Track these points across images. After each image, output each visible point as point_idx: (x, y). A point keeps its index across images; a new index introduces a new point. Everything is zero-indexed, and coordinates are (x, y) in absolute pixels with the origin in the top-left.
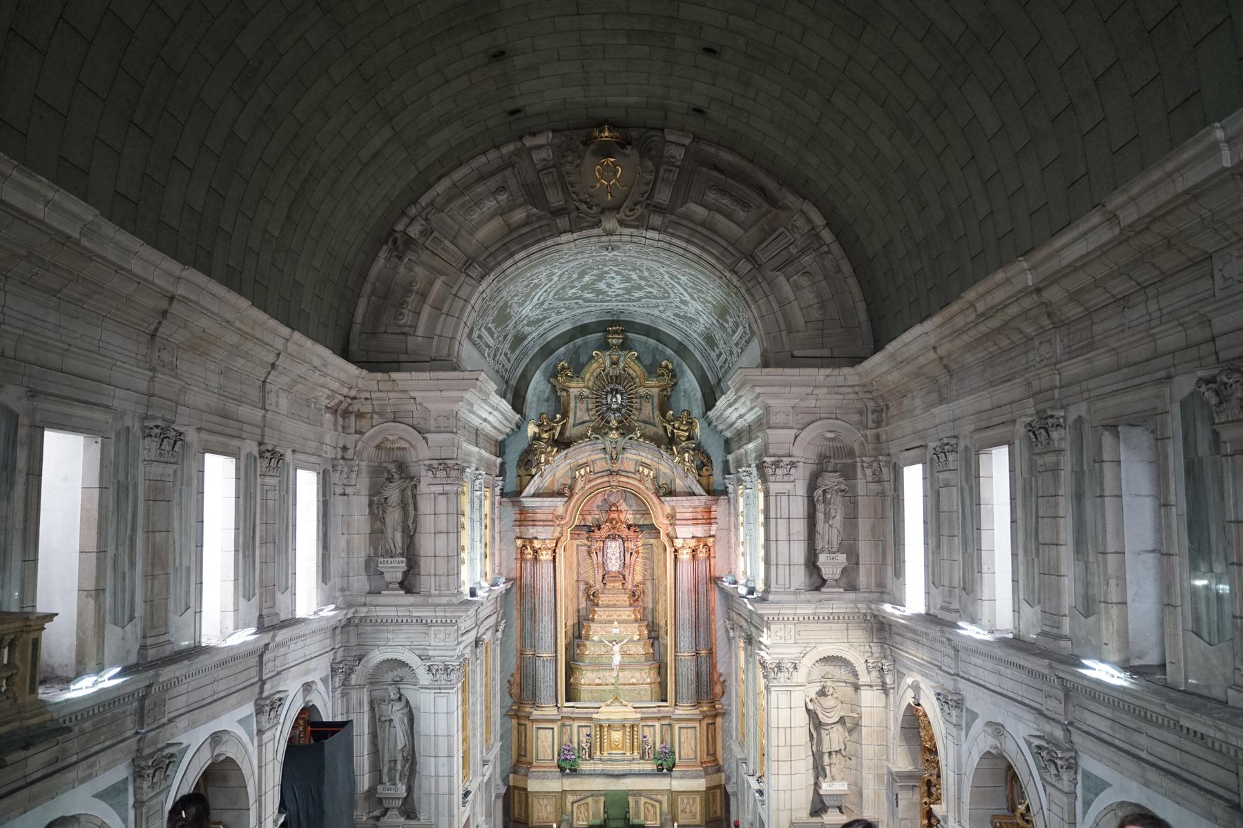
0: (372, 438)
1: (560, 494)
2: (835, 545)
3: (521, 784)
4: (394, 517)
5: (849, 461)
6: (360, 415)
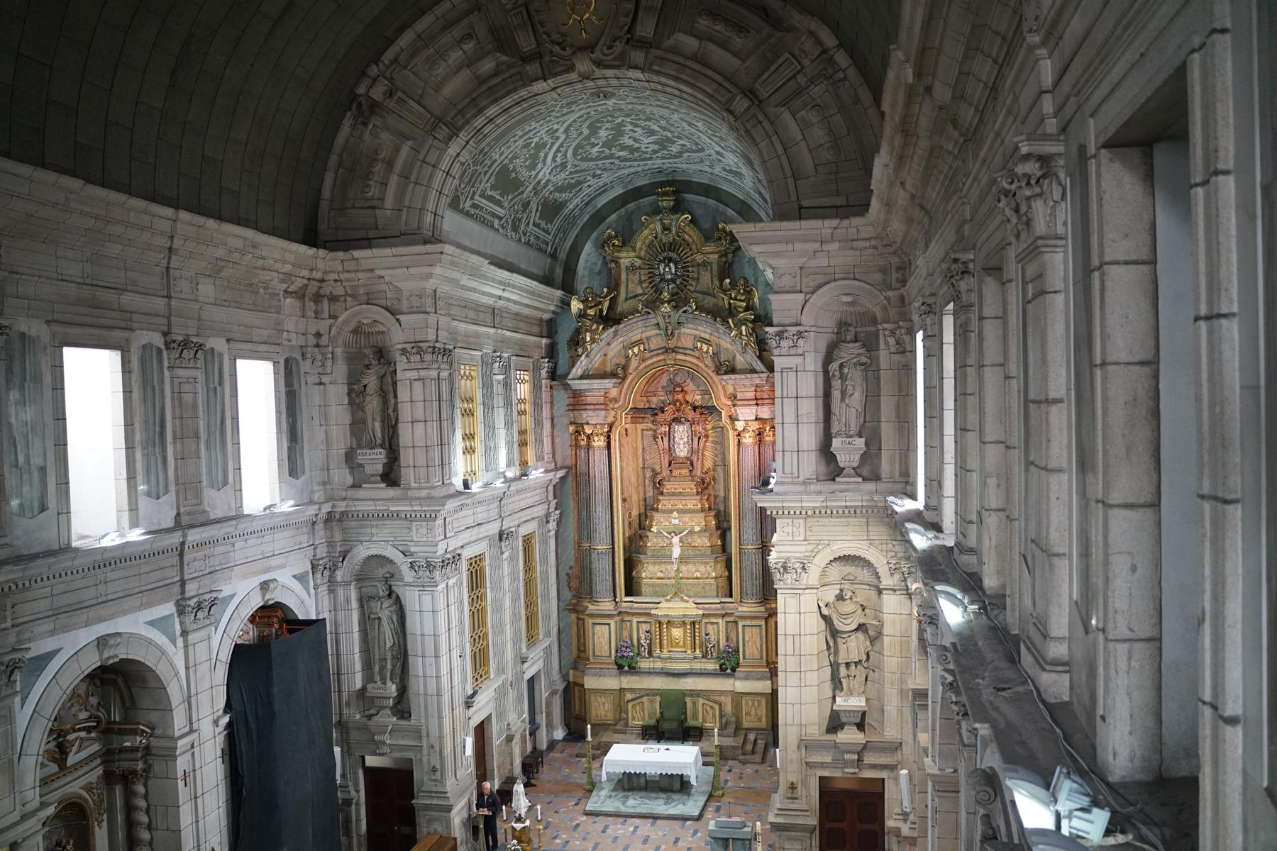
0: (346, 322)
1: (613, 375)
2: (854, 427)
3: (579, 681)
4: (373, 404)
5: (873, 329)
6: (333, 299)
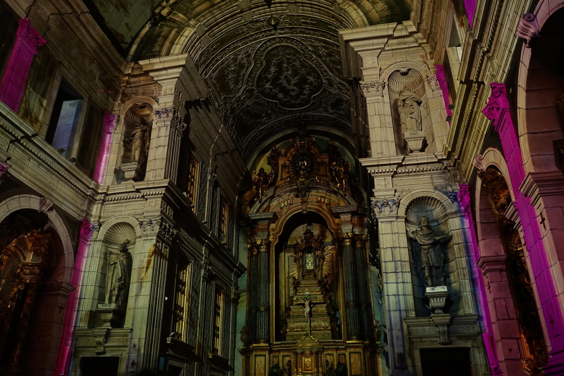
4: (137, 143)
